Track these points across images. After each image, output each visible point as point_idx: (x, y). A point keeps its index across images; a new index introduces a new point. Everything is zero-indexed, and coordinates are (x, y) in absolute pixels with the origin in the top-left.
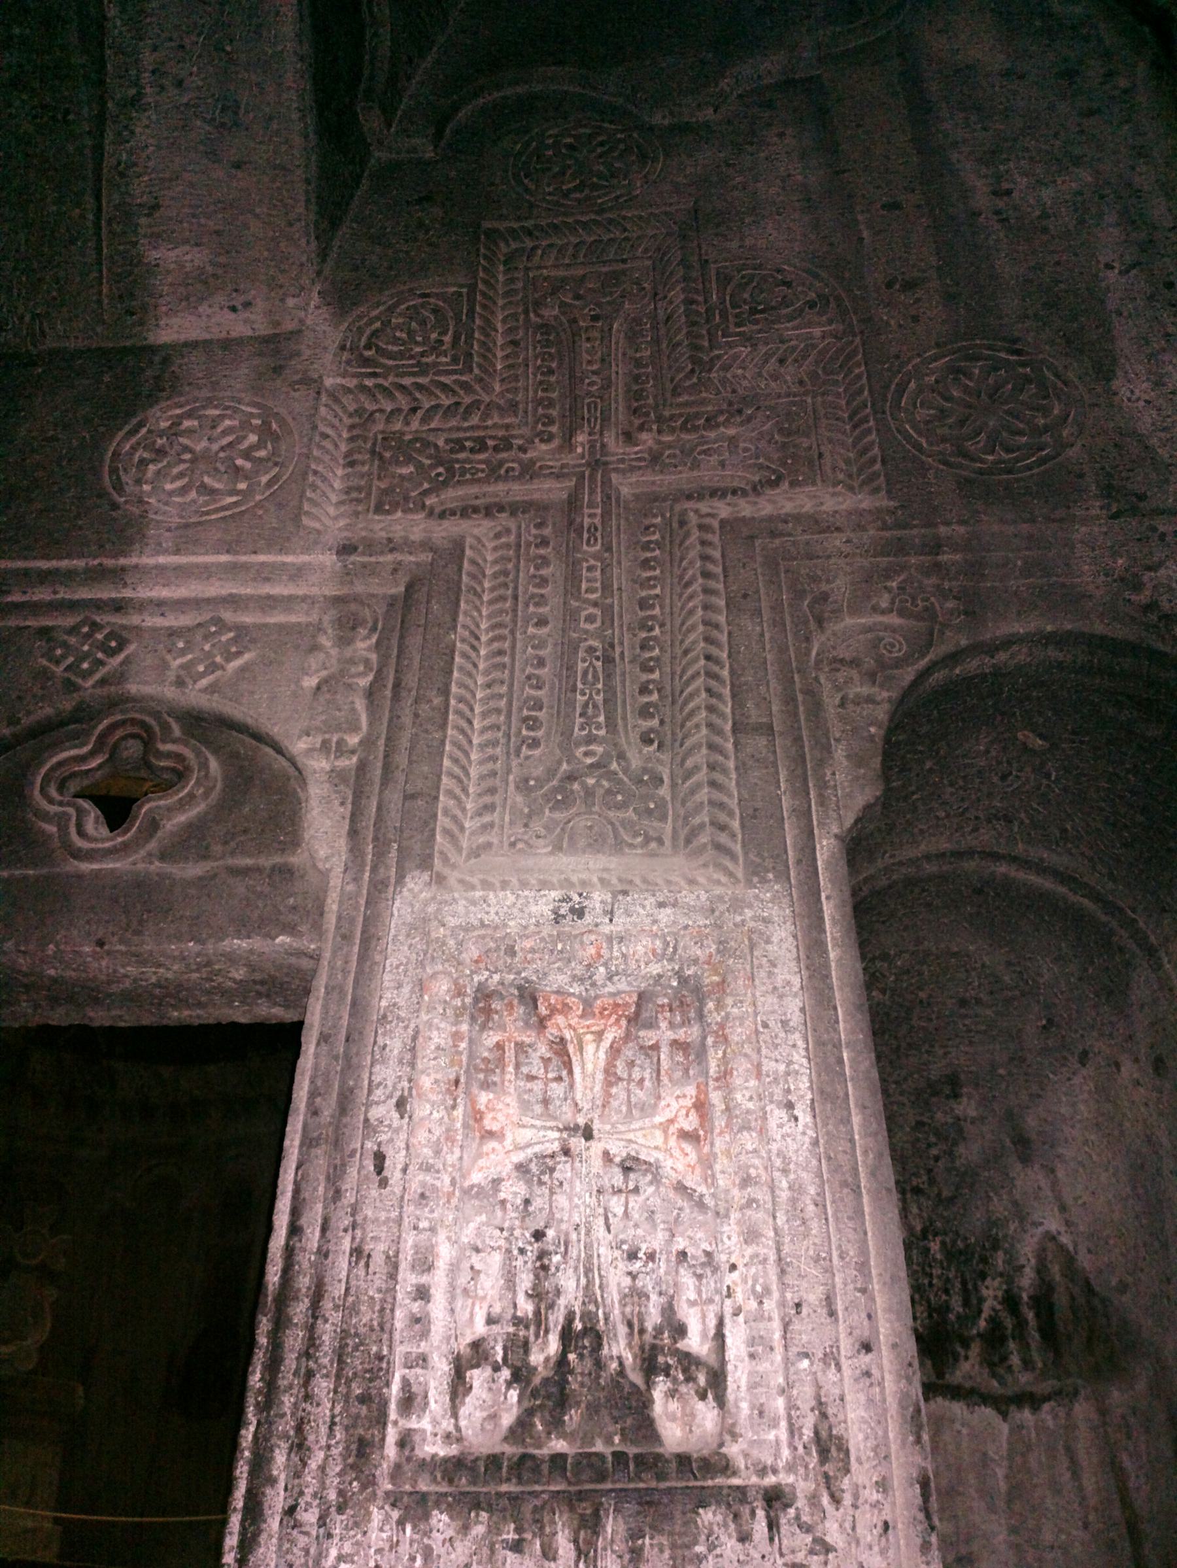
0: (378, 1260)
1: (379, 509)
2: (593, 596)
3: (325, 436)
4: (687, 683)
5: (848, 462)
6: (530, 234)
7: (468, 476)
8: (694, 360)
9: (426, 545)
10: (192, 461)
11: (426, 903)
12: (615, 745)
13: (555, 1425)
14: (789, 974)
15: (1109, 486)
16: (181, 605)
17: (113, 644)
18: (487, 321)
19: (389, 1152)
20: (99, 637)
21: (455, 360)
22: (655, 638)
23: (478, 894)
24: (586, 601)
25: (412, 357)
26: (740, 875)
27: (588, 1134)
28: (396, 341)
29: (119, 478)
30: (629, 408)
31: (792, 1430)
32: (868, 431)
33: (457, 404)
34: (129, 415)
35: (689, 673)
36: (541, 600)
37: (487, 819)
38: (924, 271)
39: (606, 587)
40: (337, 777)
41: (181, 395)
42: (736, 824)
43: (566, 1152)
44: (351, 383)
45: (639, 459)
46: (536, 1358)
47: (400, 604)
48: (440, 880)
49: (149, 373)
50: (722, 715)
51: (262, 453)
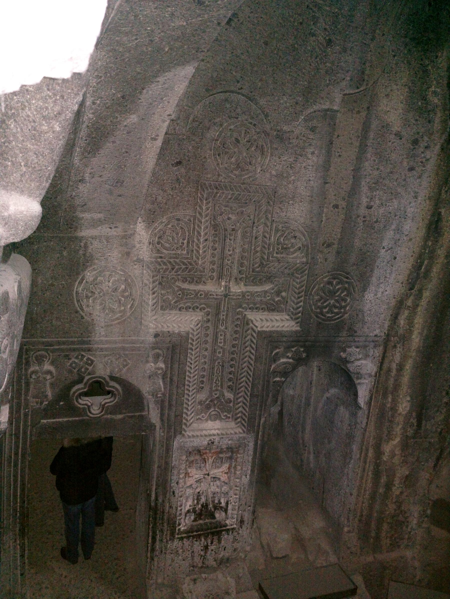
0: (174, 507)
1: (162, 308)
2: (221, 345)
3: (146, 285)
4: (242, 378)
5: (293, 308)
6: (217, 188)
7: (189, 296)
8: (262, 263)
9: (179, 334)
10: (104, 295)
11: (181, 442)
12: (223, 392)
13: (200, 519)
14: (251, 452)
15: (350, 328)
16: (106, 349)
17: (90, 362)
18: (199, 233)
19: (175, 491)
20: (85, 359)
21: (188, 253)
22: (234, 358)
23: (192, 440)
24: (219, 346)
25: (173, 250)
26: (245, 430)
27: (208, 475)
28: (168, 241)
29: (81, 305)
30: (238, 268)
31: (237, 520)
32: (301, 301)
33: (187, 268)
34: (78, 274)
35: (243, 375)
36: (206, 342)
37: (193, 414)
38: (334, 239)
39: (225, 342)
40: (156, 402)
41: (95, 264)
42: (246, 419)
43: (204, 478)
44: (153, 260)
45: (240, 295)
46: (197, 509)
47: (170, 349)
48: (183, 435)
49: (81, 252)
50: (248, 390)
51: (127, 294)
